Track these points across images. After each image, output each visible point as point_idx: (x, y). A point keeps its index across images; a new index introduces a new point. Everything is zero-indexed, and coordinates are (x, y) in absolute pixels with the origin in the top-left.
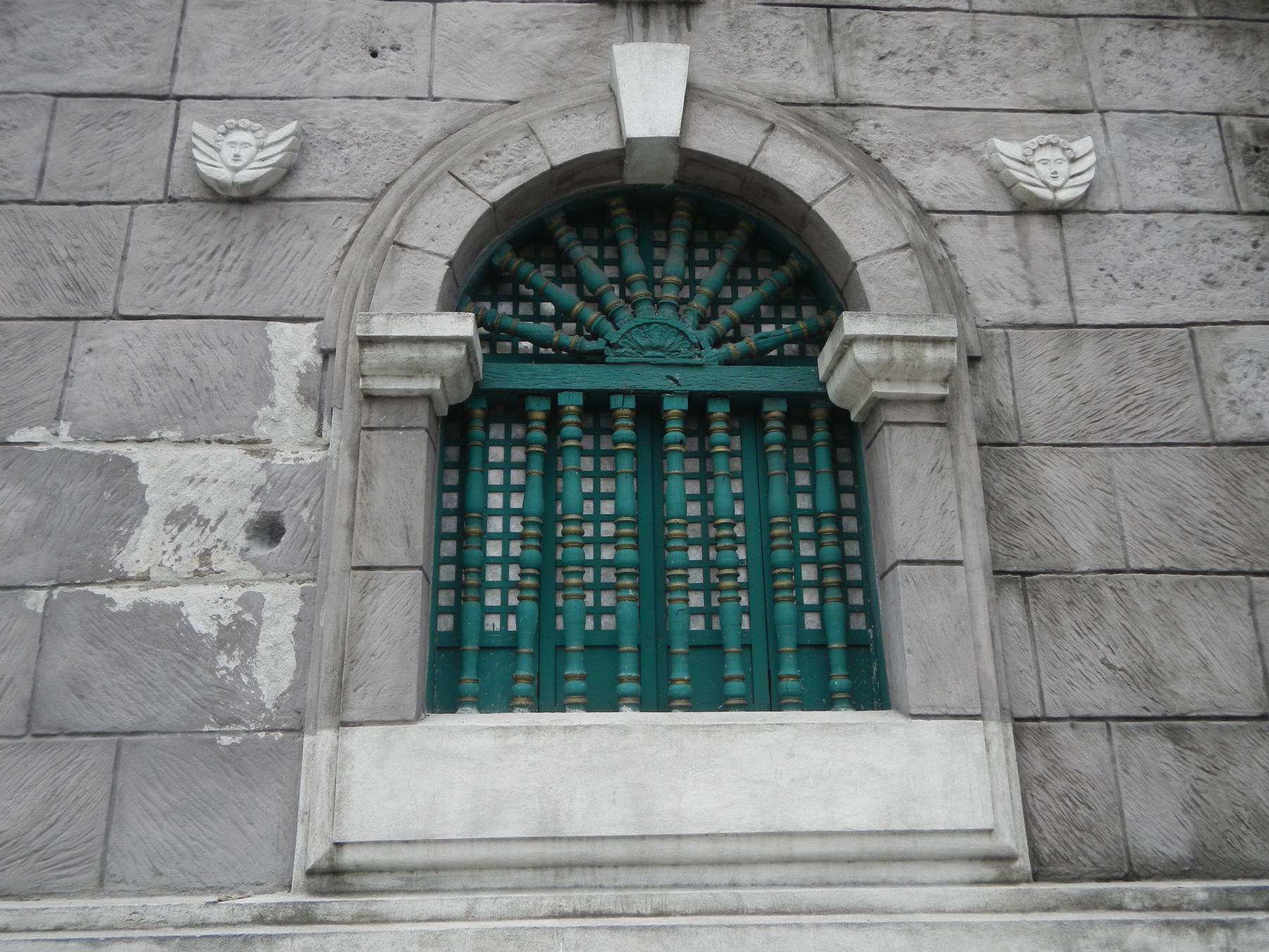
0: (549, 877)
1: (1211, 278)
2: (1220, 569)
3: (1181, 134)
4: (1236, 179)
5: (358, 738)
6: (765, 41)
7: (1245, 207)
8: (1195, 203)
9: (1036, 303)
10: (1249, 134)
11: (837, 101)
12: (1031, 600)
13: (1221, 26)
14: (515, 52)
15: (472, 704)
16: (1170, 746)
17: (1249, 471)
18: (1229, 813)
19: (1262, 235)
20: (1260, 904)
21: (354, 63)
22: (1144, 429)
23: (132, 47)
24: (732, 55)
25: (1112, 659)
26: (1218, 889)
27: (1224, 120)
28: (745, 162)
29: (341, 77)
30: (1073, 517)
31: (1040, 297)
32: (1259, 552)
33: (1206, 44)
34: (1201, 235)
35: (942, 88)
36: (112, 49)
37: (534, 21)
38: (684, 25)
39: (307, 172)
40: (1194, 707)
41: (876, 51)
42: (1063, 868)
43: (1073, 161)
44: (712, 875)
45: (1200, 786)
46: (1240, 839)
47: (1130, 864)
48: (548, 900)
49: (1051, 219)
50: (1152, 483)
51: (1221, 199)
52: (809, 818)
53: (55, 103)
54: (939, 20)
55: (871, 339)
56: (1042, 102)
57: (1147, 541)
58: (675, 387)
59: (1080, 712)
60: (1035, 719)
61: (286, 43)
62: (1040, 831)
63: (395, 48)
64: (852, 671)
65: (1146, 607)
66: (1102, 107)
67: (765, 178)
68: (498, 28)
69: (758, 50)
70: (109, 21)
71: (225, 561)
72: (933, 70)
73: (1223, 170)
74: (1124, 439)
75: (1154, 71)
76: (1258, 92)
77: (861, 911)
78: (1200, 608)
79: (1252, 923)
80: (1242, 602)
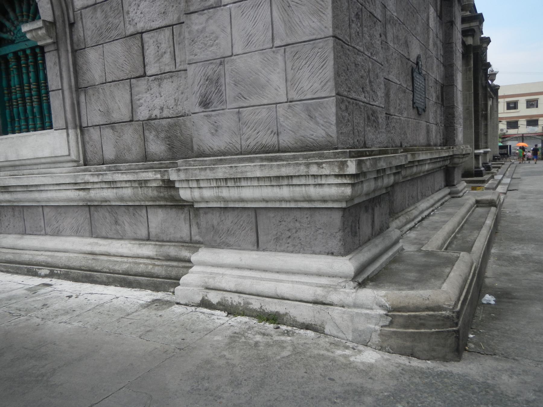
0: (13, 168)
2: (125, 78)
15: (17, 131)
16: (112, 131)
22: (111, 36)
32: (133, 71)
40: (116, 120)
42: (92, 163)
44: (35, 167)
45: (117, 141)
48: (9, 173)
52: (40, 155)
59: (94, 124)
65: (108, 93)
74: (107, 41)
77: (50, 174)
79: (106, 174)
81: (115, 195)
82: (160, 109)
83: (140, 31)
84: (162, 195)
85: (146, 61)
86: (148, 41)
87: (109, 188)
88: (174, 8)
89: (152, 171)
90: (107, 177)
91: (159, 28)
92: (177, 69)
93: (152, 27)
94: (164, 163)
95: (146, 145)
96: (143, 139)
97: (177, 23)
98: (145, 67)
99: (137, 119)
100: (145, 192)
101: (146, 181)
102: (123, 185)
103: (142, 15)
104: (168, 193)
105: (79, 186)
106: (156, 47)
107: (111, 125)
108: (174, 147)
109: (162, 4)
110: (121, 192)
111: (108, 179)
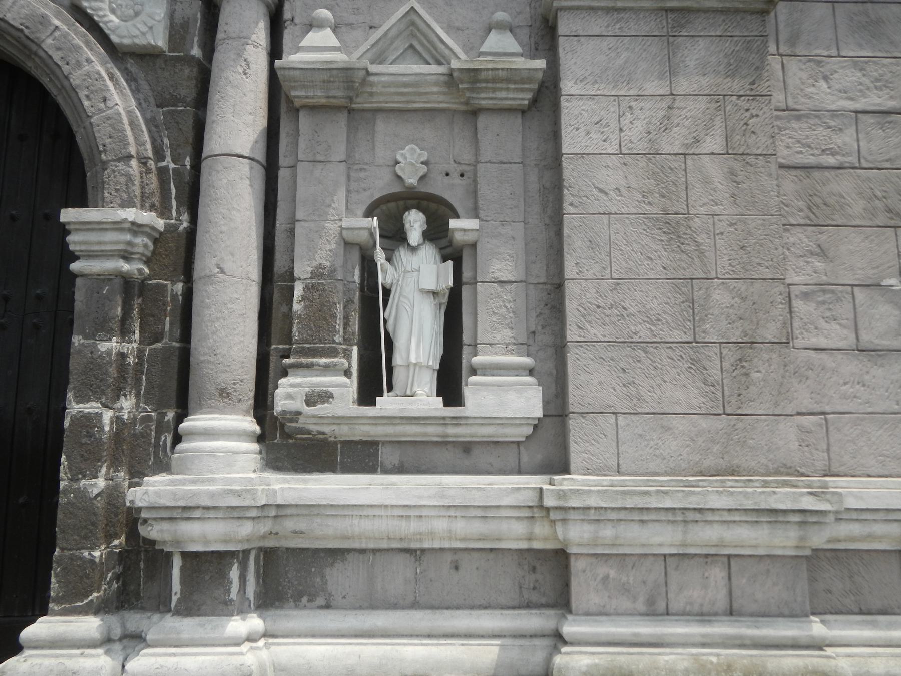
36: (876, 87)
53: (856, 116)
70: (871, 71)
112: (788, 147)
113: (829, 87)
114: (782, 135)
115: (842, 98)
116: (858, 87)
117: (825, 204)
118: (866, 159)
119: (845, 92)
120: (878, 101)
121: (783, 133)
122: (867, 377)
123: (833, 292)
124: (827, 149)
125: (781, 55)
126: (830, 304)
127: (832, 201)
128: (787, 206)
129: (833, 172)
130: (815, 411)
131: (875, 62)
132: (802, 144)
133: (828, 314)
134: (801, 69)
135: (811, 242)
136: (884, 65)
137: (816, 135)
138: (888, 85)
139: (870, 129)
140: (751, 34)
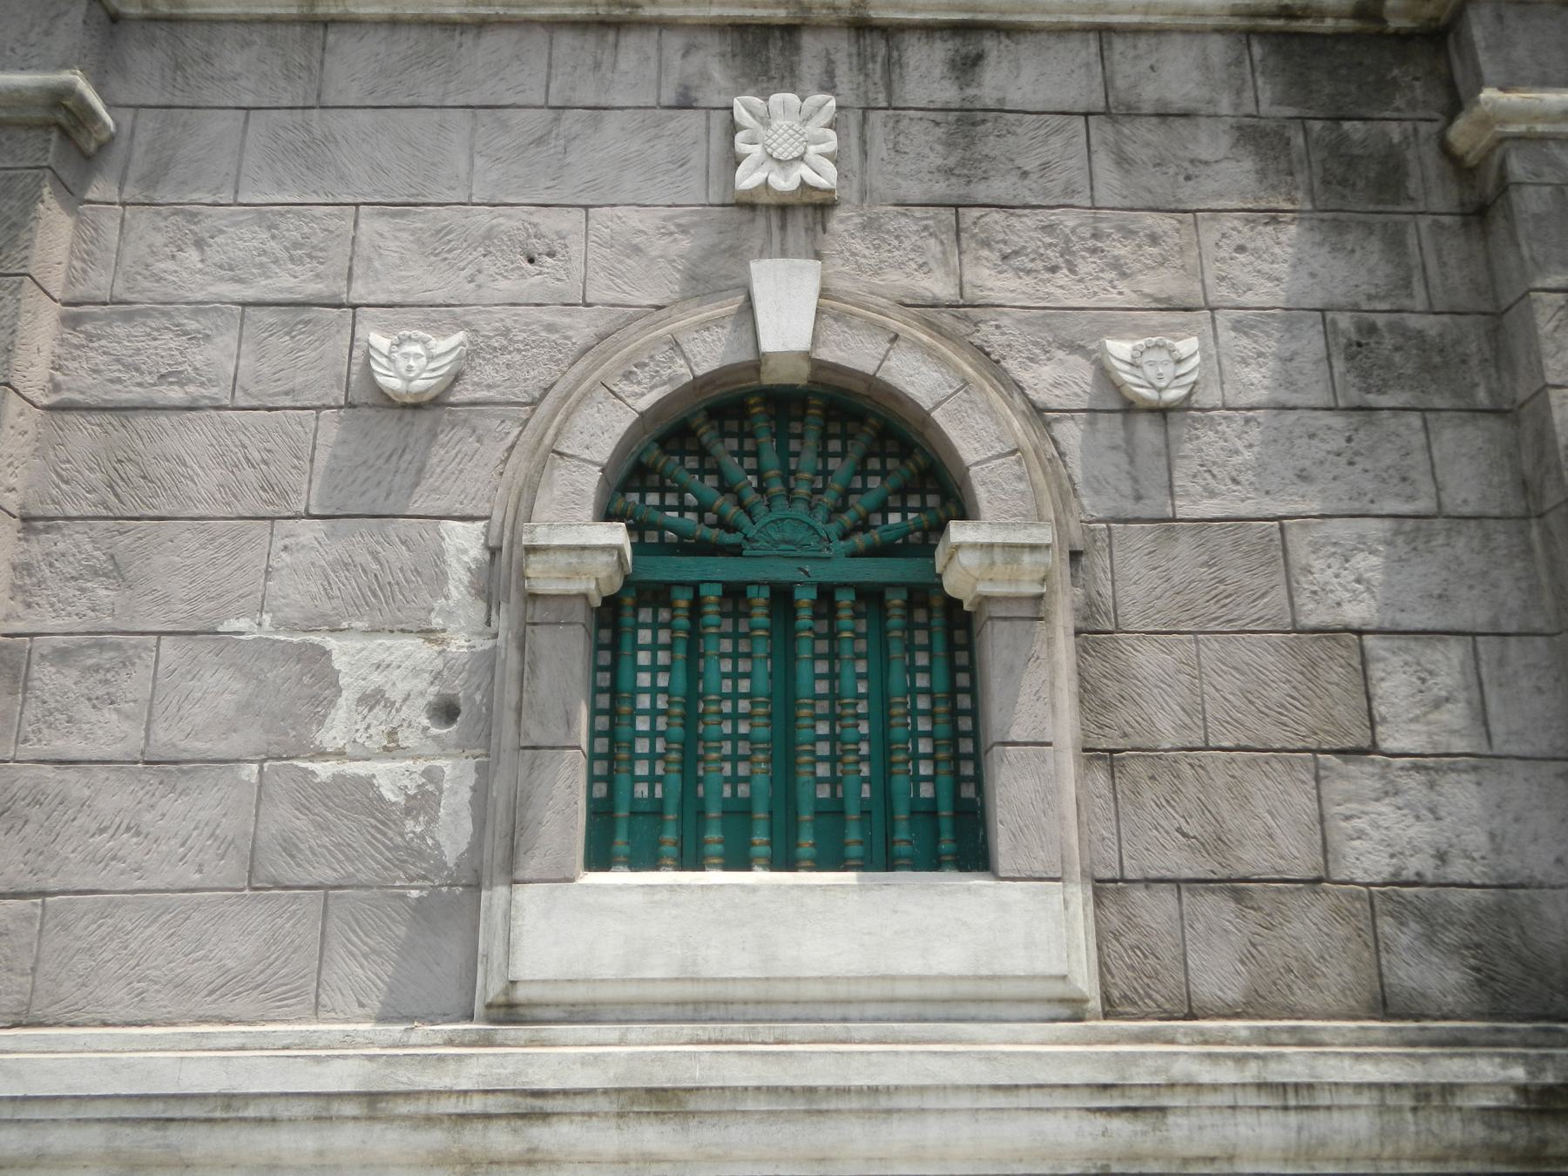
1: (1304, 473)
2: (1291, 747)
3: (1287, 330)
4: (1336, 375)
5: (525, 893)
6: (896, 243)
7: (1341, 403)
8: (1295, 399)
9: (1139, 498)
10: (1352, 330)
11: (961, 302)
12: (1117, 774)
13: (1335, 219)
14: (661, 257)
15: (623, 863)
16: (1233, 905)
17: (1324, 657)
18: (1280, 963)
19: (1356, 430)
20: (1294, 1041)
21: (512, 270)
22: (1230, 617)
23: (310, 256)
24: (864, 256)
25: (1186, 828)
26: (1258, 1027)
27: (1329, 315)
28: (871, 372)
29: (503, 284)
30: (1160, 699)
31: (1142, 492)
33: (1318, 237)
34: (1298, 431)
35: (1061, 287)
36: (292, 259)
37: (678, 226)
38: (819, 227)
39: (471, 377)
41: (1000, 251)
43: (1179, 362)
44: (826, 1011)
46: (1289, 987)
47: (1190, 1006)
49: (1158, 417)
50: (1235, 668)
51: (1319, 396)
52: (910, 964)
53: (243, 312)
54: (1062, 218)
55: (975, 546)
56: (1157, 300)
57: (1228, 722)
58: (804, 578)
59: (1153, 874)
60: (1114, 881)
61: (450, 251)
62: (1113, 977)
63: (551, 254)
64: (957, 838)
65: (1219, 782)
66: (1215, 304)
67: (888, 385)
68: (645, 233)
69: (889, 251)
70: (288, 230)
71: (408, 739)
72: (1054, 269)
73: (1324, 366)
74: (1211, 626)
75: (1266, 267)
76: (1365, 286)
78: (1269, 783)
79: (1281, 1056)
80: (1307, 777)
81: (1293, 1135)
82: (1432, 856)
83: (1356, 625)
84: (1505, 1137)
85: (1380, 709)
86: (1383, 659)
87: (1265, 1108)
88: (1475, 592)
89: (1491, 1056)
90: (1286, 1067)
91: (1424, 632)
92: (1496, 751)
93: (1398, 625)
94: (1513, 1031)
95: (1384, 962)
96: (1371, 944)
97: (1490, 631)
98: (1372, 728)
99: (1343, 877)
100: (1435, 1128)
101: (1448, 1089)
102: (1346, 1098)
103: (1360, 587)
104: (1531, 1132)
105: (1123, 1096)
106: (1414, 679)
107: (1235, 887)
108: (1497, 976)
109: (1434, 573)
110: (1318, 1124)
111: (1291, 1074)
112: (95, 371)
113: (202, 261)
114: (91, 349)
115: (221, 279)
116: (257, 259)
117: (144, 478)
118: (246, 392)
119: (231, 269)
120: (290, 282)
121: (96, 345)
122: (148, 817)
123: (118, 647)
124: (171, 374)
125: (124, 204)
126: (108, 670)
127: (157, 470)
128: (66, 482)
129: (175, 418)
130: (25, 889)
131: (298, 214)
132: (124, 365)
133: (101, 691)
134: (157, 229)
135: (99, 549)
136: (314, 218)
137: (156, 348)
138: (314, 254)
139: (264, 335)
140: (20, 164)
